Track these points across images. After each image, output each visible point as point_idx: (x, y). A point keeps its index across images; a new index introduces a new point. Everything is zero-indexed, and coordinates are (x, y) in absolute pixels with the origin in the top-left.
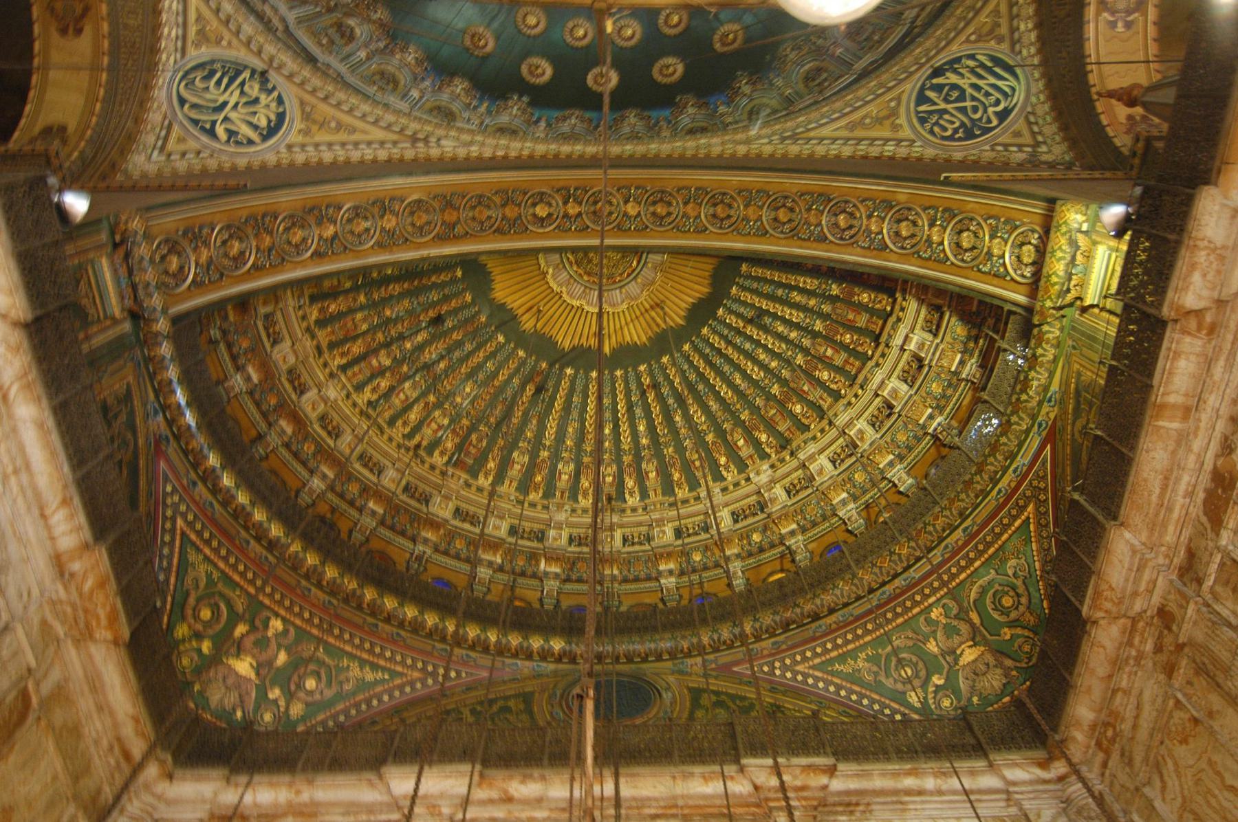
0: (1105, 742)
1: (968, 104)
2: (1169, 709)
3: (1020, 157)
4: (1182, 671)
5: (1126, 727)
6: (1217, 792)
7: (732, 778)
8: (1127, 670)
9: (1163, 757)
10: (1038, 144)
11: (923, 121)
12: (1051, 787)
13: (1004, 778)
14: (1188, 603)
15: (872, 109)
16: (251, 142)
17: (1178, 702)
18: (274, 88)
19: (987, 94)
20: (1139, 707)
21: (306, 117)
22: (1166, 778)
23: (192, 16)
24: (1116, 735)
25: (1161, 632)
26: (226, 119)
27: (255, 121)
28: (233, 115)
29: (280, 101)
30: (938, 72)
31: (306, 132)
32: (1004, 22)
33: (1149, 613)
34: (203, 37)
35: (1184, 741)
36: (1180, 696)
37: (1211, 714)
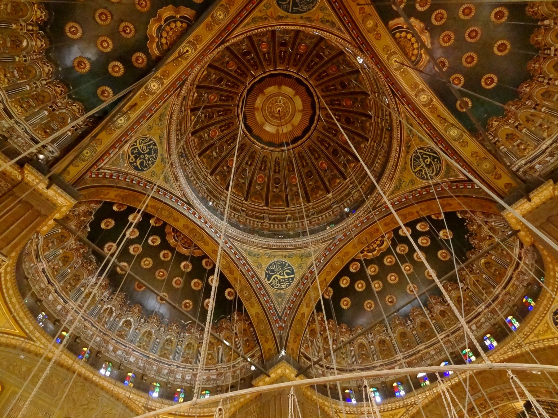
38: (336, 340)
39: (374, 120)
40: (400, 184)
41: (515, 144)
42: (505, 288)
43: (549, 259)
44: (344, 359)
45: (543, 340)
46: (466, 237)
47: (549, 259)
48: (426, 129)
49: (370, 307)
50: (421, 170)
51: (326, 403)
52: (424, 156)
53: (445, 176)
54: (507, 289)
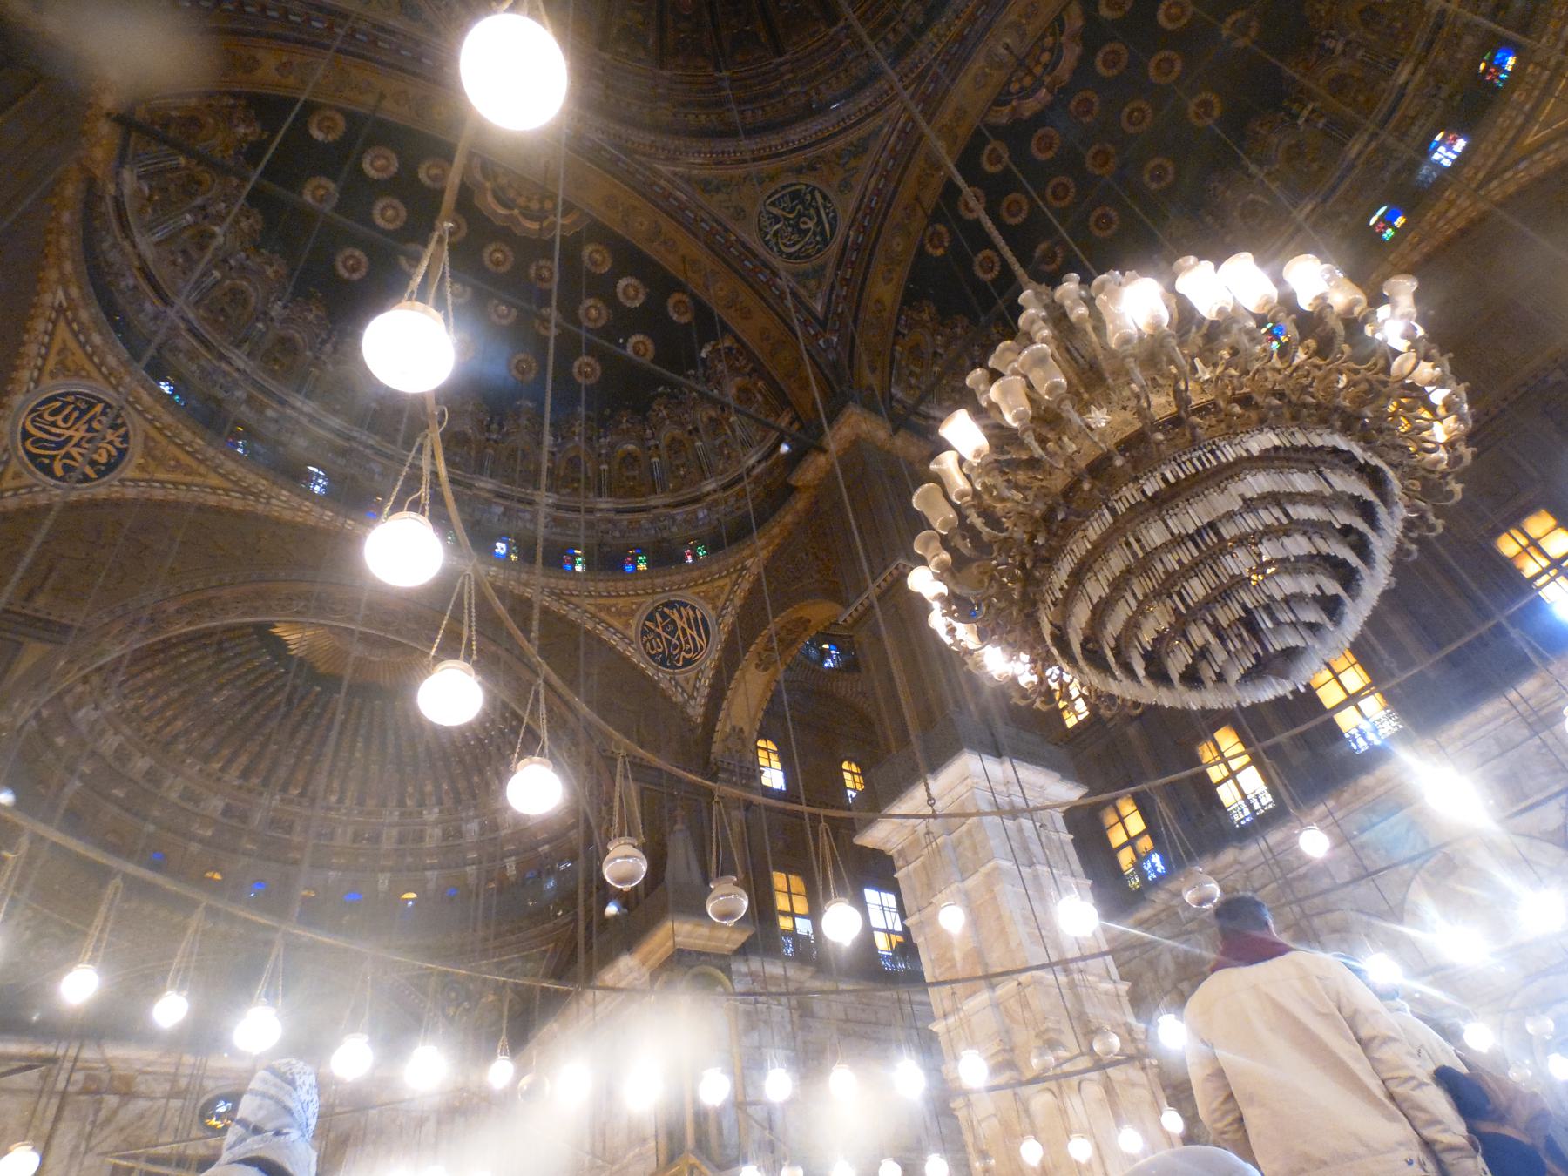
1: (674, 641)
3: (679, 698)
10: (692, 697)
11: (644, 633)
15: (621, 602)
16: (86, 479)
18: (124, 424)
19: (687, 642)
21: (148, 453)
23: (57, 346)
26: (68, 456)
27: (96, 457)
28: (75, 452)
29: (125, 438)
30: (670, 605)
31: (141, 468)
32: (723, 597)
34: (63, 368)
38: (205, 217)
39: (782, 64)
40: (718, 190)
41: (912, 367)
42: (618, 511)
43: (776, 530)
44: (174, 263)
45: (602, 621)
46: (660, 389)
47: (776, 530)
48: (871, 187)
49: (353, 270)
50: (777, 220)
51: (68, 267)
52: (812, 212)
53: (795, 275)
54: (618, 517)
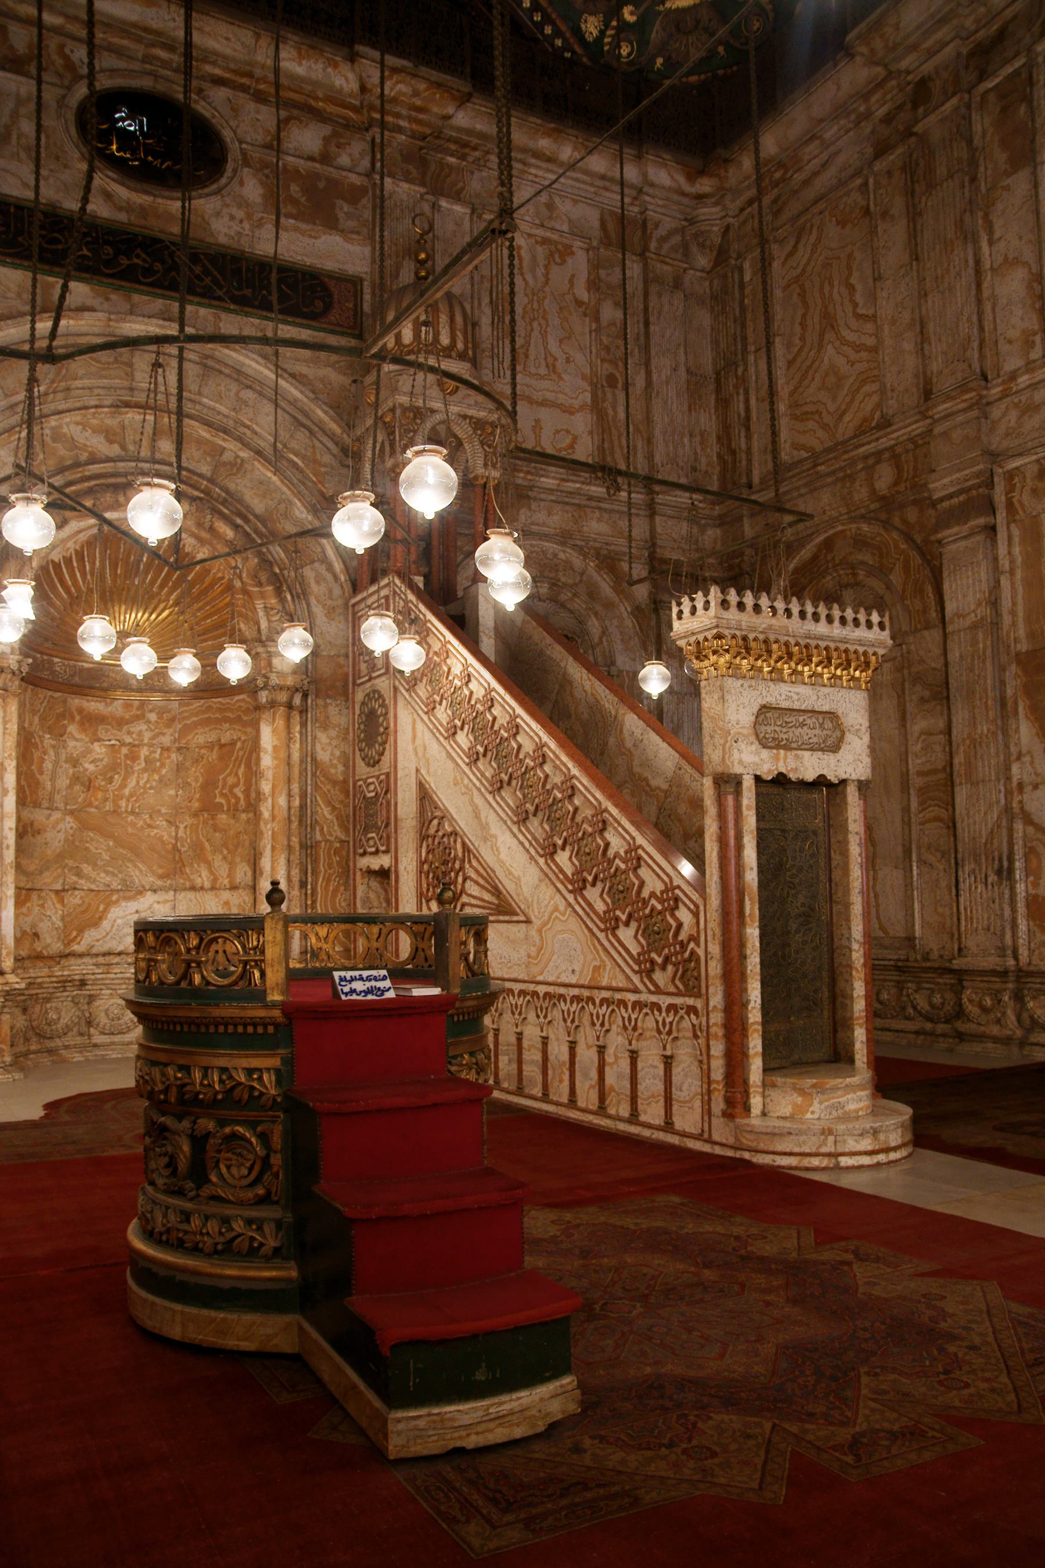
0: (767, 181)
2: (851, 186)
4: (892, 157)
5: (799, 177)
6: (836, 283)
7: (336, 65)
8: (842, 122)
9: (812, 226)
12: (685, 201)
13: (645, 175)
14: (954, 94)
17: (866, 184)
20: (824, 166)
22: (801, 246)
24: (783, 180)
25: (903, 104)
33: (910, 78)
35: (842, 224)
36: (871, 181)
37: (885, 214)
